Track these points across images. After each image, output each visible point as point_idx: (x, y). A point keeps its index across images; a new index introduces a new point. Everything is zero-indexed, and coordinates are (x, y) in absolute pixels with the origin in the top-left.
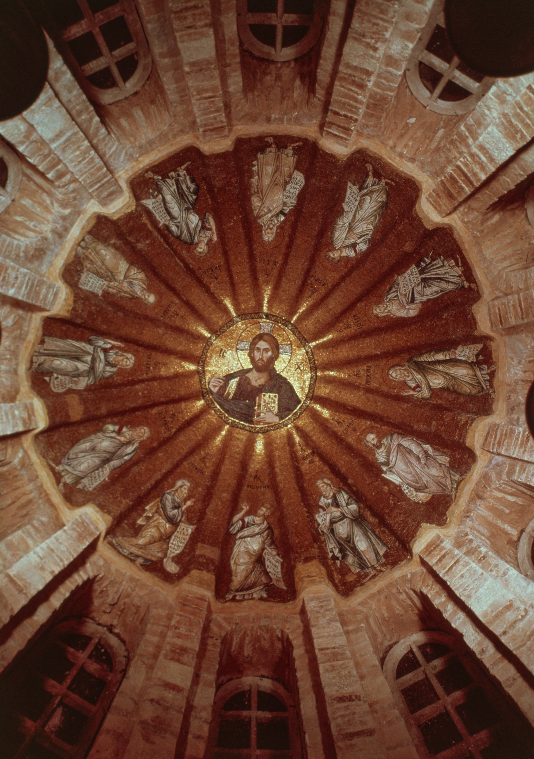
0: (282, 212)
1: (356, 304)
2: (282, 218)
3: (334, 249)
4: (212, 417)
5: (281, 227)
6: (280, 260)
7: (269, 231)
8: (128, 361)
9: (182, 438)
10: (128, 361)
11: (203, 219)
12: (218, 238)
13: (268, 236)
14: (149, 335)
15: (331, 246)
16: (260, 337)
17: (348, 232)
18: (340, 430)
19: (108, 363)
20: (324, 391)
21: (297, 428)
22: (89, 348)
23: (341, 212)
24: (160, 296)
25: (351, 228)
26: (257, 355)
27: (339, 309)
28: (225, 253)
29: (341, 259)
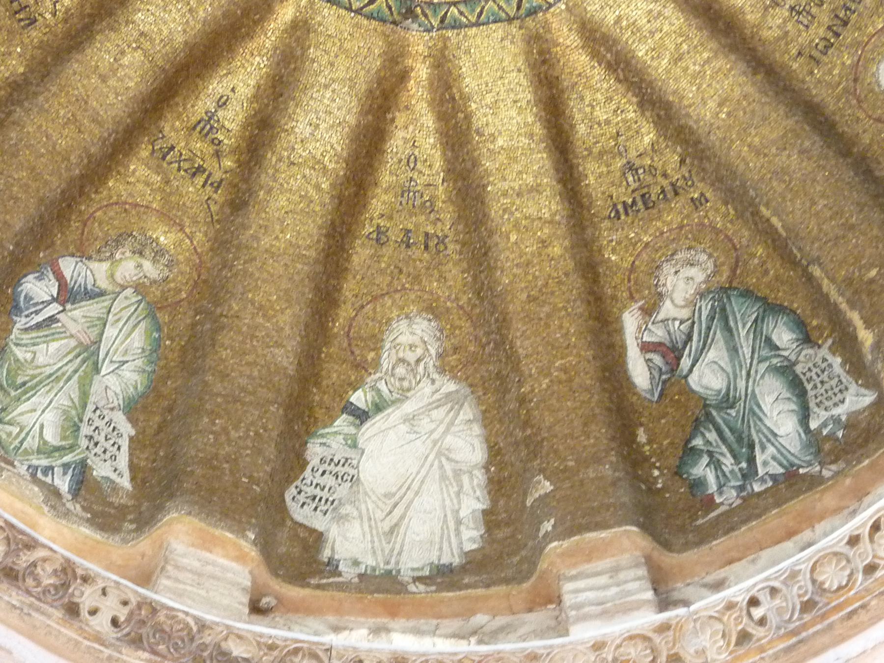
0: (361, 416)
1: (30, 70)
2: (359, 398)
3: (139, 288)
5: (363, 367)
6: (360, 254)
7: (411, 357)
11: (672, 381)
12: (619, 320)
13: (412, 336)
15: (156, 303)
17: (98, 342)
23: (134, 409)
25: (90, 355)
27: (103, 51)
28: (590, 267)
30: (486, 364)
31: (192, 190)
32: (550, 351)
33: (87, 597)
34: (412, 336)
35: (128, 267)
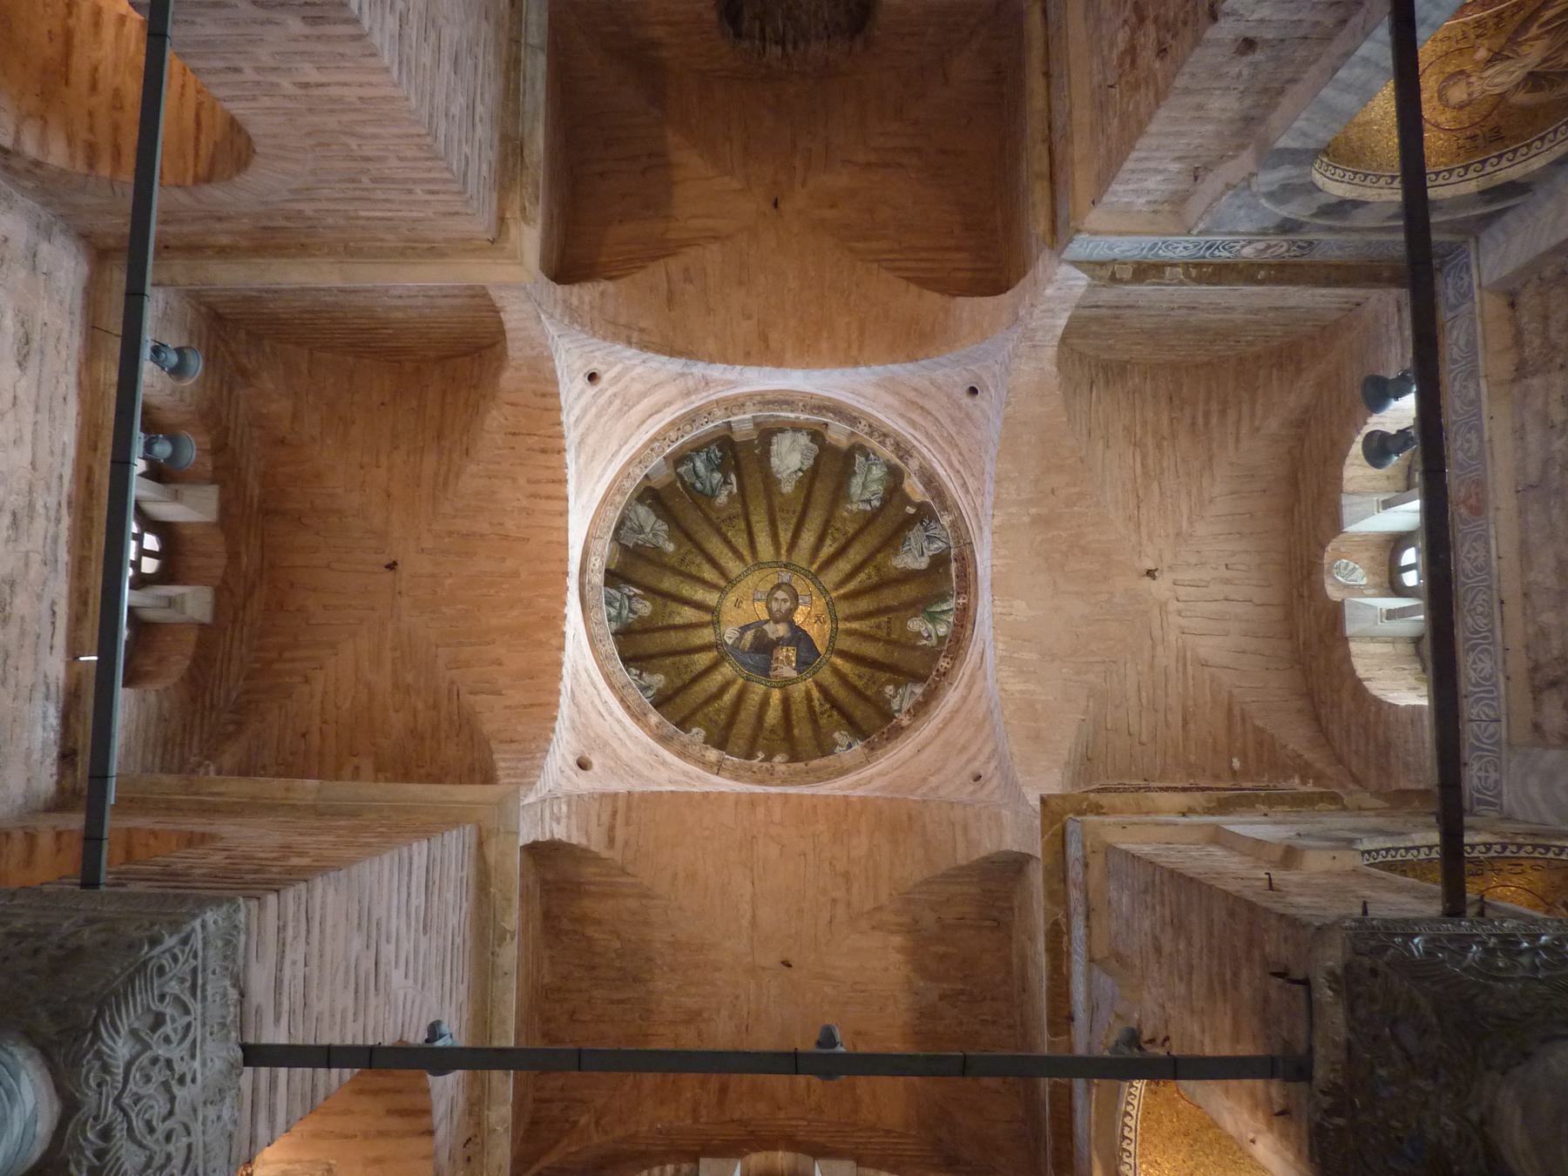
4: (727, 670)
5: (800, 481)
6: (799, 508)
8: (645, 608)
9: (697, 688)
10: (645, 608)
13: (787, 488)
14: (668, 583)
15: (848, 498)
16: (778, 587)
18: (860, 684)
19: (631, 610)
20: (845, 643)
21: (817, 684)
22: (618, 595)
24: (679, 546)
25: (864, 486)
26: (775, 606)
27: (859, 558)
28: (745, 504)
29: (860, 511)
30: (770, 481)
31: (839, 525)
32: (755, 483)
33: (867, 429)
34: (787, 488)
35: (854, 507)
